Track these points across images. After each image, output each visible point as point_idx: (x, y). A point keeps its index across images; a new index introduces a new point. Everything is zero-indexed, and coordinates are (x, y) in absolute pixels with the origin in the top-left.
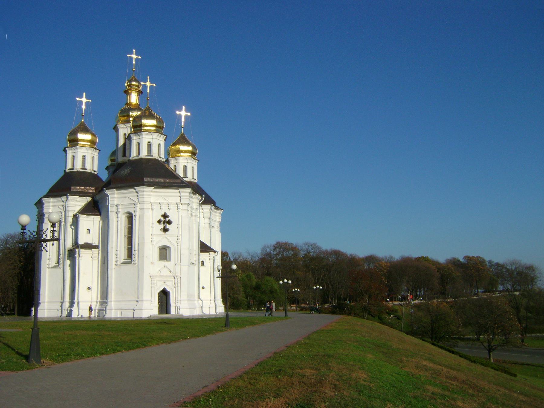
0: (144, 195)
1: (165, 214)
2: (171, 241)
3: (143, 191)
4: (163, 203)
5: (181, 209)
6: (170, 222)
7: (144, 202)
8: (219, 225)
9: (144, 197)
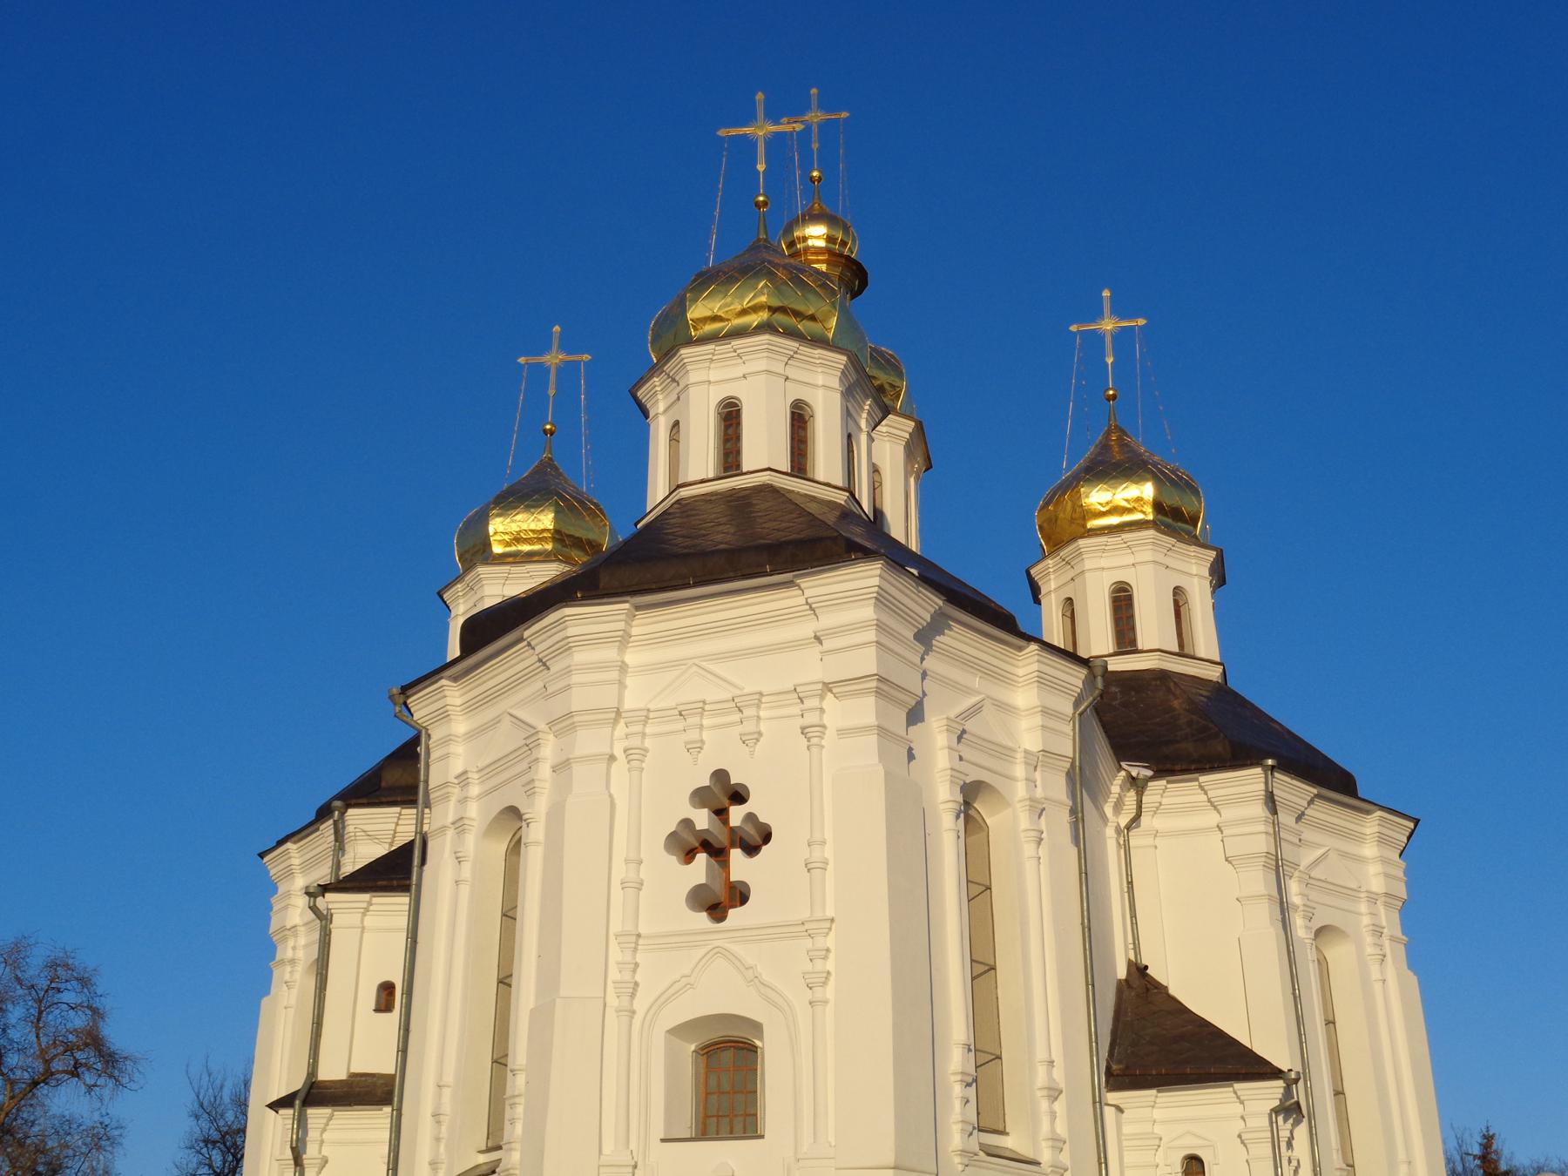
0: (568, 671)
1: (720, 776)
2: (766, 977)
3: (565, 648)
4: (702, 708)
5: (830, 733)
6: (756, 840)
7: (570, 715)
8: (1390, 921)
9: (568, 687)
